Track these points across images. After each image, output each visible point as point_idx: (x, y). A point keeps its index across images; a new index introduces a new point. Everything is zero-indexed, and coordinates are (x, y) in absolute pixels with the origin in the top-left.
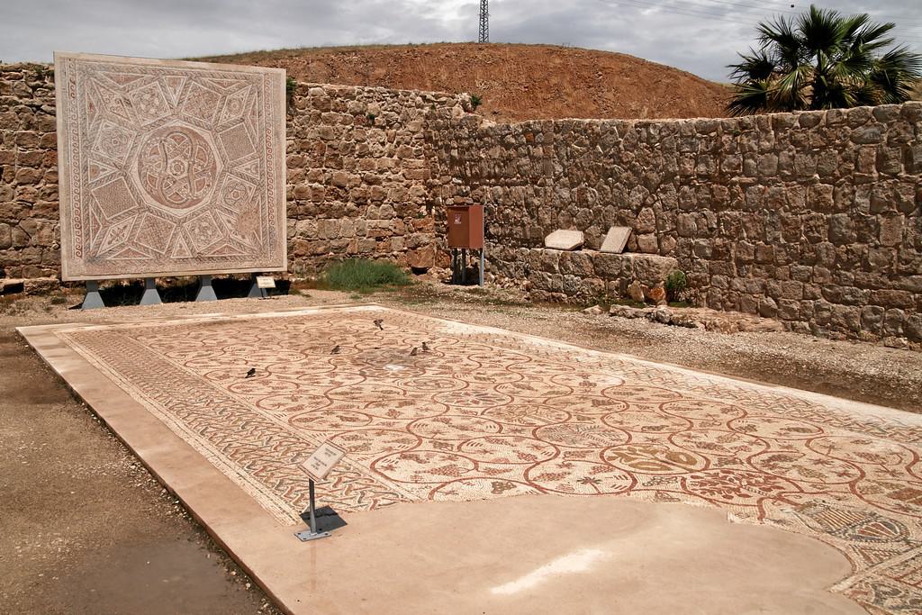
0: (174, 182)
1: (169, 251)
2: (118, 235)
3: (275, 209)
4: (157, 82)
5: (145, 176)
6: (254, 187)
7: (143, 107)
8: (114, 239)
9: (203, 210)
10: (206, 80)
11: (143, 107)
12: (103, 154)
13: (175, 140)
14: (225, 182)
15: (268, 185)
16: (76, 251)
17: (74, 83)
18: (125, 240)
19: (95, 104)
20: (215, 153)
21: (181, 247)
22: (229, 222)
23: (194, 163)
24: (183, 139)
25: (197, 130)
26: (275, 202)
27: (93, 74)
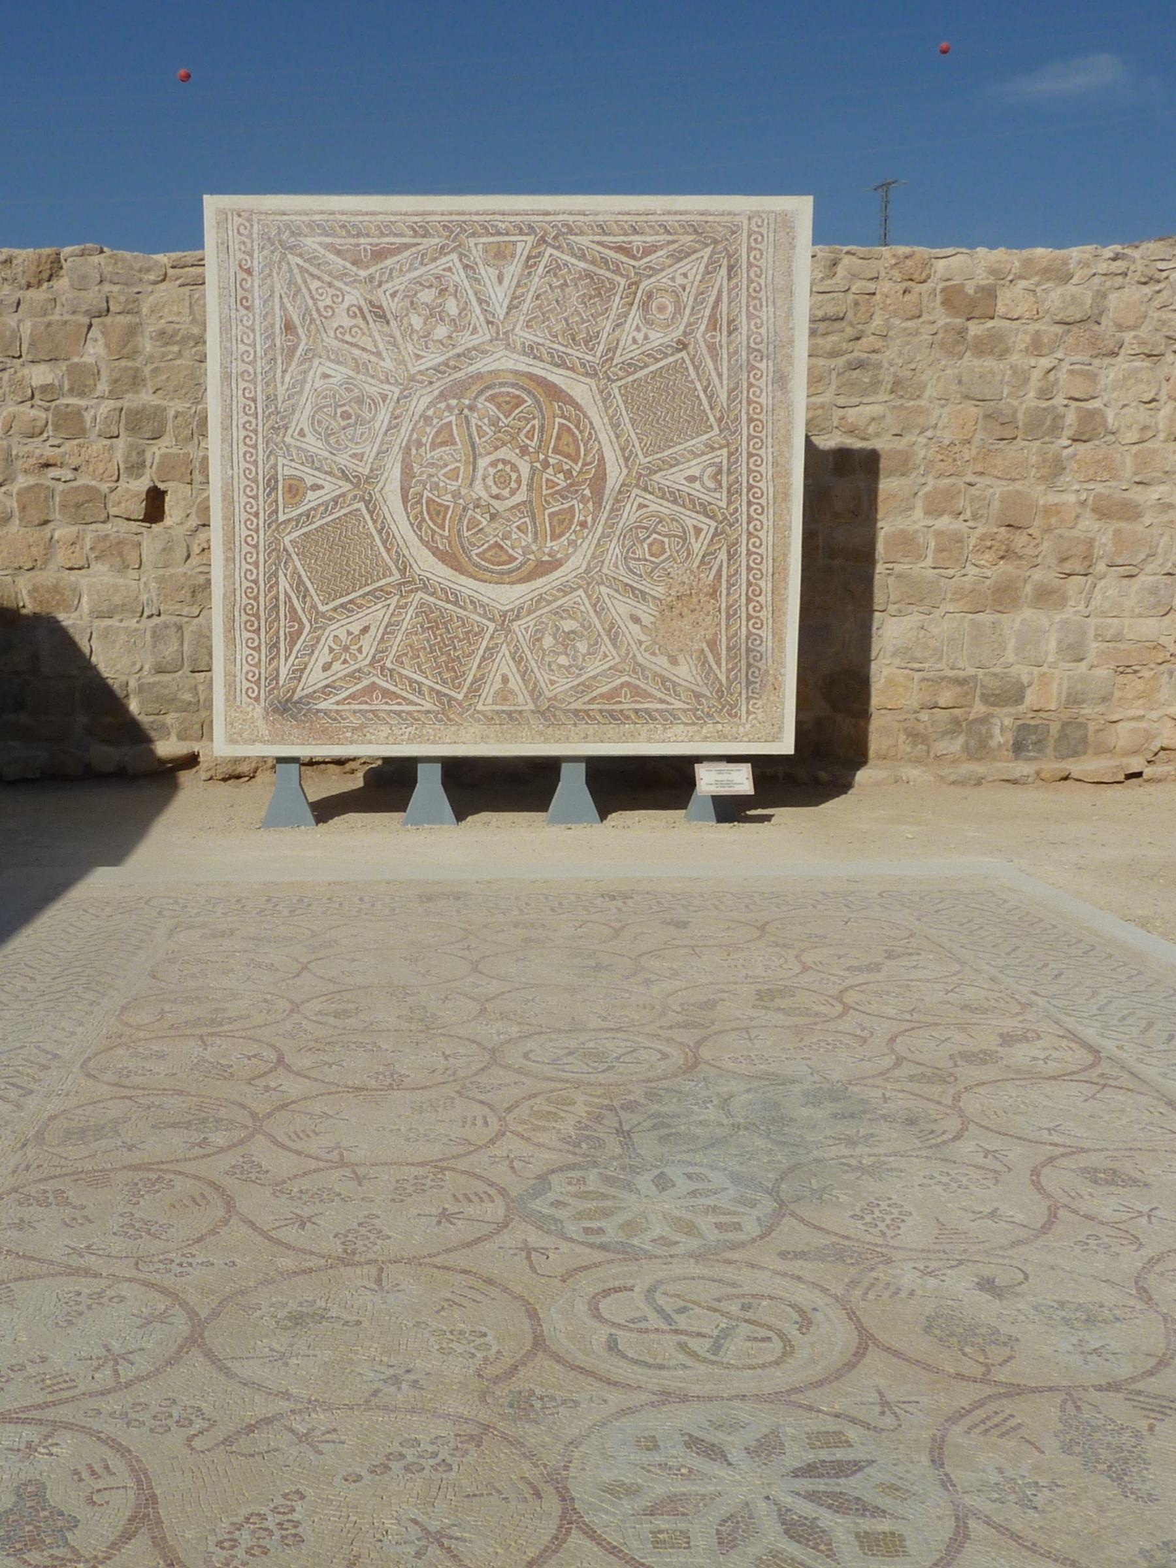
0: (493, 517)
1: (475, 690)
2: (346, 649)
3: (766, 585)
4: (454, 256)
5: (419, 502)
6: (709, 526)
7: (417, 321)
8: (334, 659)
9: (565, 590)
10: (584, 241)
11: (417, 321)
12: (314, 444)
13: (499, 406)
14: (629, 514)
15: (750, 519)
16: (246, 685)
17: (249, 272)
18: (363, 662)
19: (297, 321)
20: (603, 437)
21: (505, 680)
22: (636, 620)
23: (546, 464)
24: (520, 402)
25: (557, 377)
26: (767, 566)
27: (291, 248)
